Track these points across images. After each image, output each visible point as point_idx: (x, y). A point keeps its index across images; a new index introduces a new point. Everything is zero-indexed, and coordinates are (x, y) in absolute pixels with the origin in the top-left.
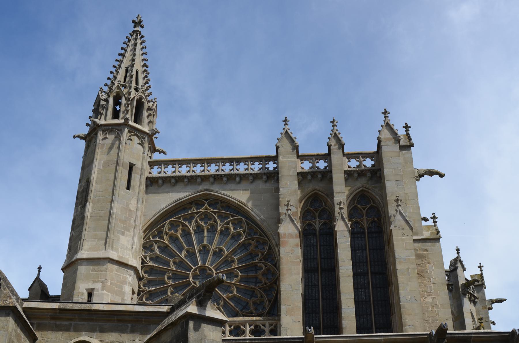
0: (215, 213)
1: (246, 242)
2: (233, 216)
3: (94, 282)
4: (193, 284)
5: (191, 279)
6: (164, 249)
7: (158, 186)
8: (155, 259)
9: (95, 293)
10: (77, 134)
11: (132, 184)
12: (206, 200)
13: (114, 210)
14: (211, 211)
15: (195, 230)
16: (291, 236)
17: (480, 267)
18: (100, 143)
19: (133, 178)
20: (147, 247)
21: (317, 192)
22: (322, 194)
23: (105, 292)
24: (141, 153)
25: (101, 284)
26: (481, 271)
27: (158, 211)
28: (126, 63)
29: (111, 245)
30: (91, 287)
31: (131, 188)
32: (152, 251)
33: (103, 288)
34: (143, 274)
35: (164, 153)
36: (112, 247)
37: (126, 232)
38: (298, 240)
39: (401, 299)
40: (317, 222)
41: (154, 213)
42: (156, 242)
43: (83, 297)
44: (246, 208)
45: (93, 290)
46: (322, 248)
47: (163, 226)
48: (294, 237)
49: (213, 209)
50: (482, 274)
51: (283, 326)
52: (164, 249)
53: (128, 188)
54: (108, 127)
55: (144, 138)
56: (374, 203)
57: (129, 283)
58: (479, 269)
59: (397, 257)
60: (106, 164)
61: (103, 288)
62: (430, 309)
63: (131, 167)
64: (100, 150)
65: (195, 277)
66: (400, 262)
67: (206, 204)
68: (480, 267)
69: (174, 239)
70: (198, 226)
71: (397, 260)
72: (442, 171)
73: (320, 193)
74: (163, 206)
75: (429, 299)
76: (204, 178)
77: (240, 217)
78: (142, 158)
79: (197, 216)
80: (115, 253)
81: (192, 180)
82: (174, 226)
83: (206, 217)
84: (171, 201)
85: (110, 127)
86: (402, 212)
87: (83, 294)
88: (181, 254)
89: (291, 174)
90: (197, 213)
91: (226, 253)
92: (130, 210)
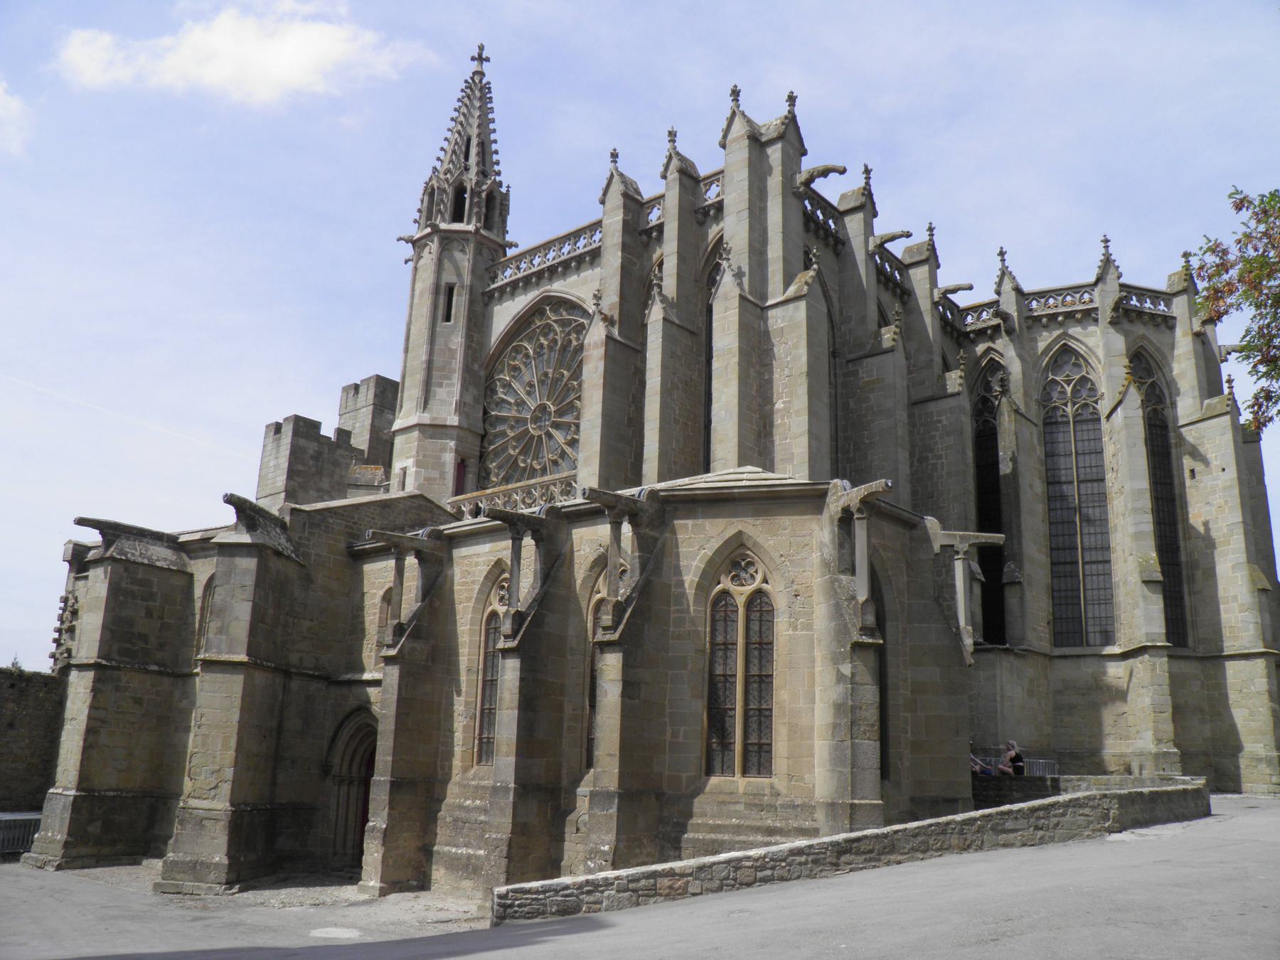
3: (407, 458)
14: (554, 321)
16: (596, 346)
31: (453, 317)
35: (516, 246)
37: (445, 382)
38: (602, 351)
45: (406, 468)
47: (505, 357)
53: (448, 318)
55: (468, 240)
57: (451, 449)
70: (541, 346)
72: (839, 163)
76: (539, 275)
77: (582, 320)
79: (538, 331)
81: (527, 282)
82: (517, 350)
84: (512, 316)
92: (450, 350)
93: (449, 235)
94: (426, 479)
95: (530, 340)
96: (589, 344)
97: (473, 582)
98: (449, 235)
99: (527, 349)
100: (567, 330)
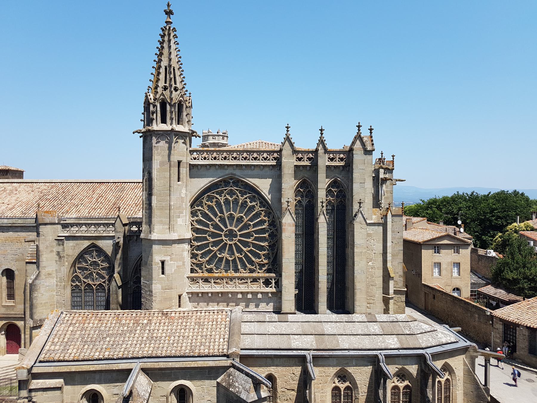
0: (237, 190)
1: (258, 213)
2: (249, 193)
3: (165, 255)
4: (225, 241)
5: (224, 238)
6: (205, 215)
7: (198, 169)
8: (199, 222)
9: (166, 263)
10: (135, 130)
11: (181, 177)
12: (231, 179)
13: (172, 203)
15: (224, 202)
16: (289, 225)
17: (393, 156)
18: (155, 146)
19: (181, 172)
20: (193, 214)
21: (306, 178)
22: (310, 181)
23: (172, 262)
24: (185, 149)
25: (169, 257)
26: (393, 159)
27: (199, 188)
28: (164, 63)
29: (173, 229)
30: (163, 259)
31: (181, 179)
32: (197, 216)
33: (171, 260)
34: (193, 233)
36: (174, 231)
39: (355, 272)
40: (304, 200)
42: (199, 210)
43: (159, 266)
44: (258, 189)
46: (306, 218)
48: (292, 225)
49: (237, 187)
50: (393, 161)
51: (283, 286)
52: (205, 215)
54: (159, 132)
56: (342, 188)
57: (186, 249)
58: (392, 157)
59: (355, 243)
60: (162, 164)
61: (171, 260)
62: (370, 270)
63: (179, 162)
64: (156, 151)
65: (226, 236)
66: (357, 247)
67: (231, 183)
68: (393, 156)
69: (210, 208)
70: (227, 199)
71: (355, 245)
73: (307, 180)
74: (202, 185)
75: (370, 263)
78: (186, 153)
80: (176, 234)
83: (231, 193)
85: (161, 132)
86: (362, 212)
87: (158, 263)
88: (216, 218)
89: (290, 173)
90: (226, 190)
91: (246, 220)
92: (182, 197)
93: (178, 133)
94: (177, 267)
95: (220, 194)
96: (285, 223)
97: (328, 376)
98: (178, 133)
99: (217, 198)
100: (245, 196)
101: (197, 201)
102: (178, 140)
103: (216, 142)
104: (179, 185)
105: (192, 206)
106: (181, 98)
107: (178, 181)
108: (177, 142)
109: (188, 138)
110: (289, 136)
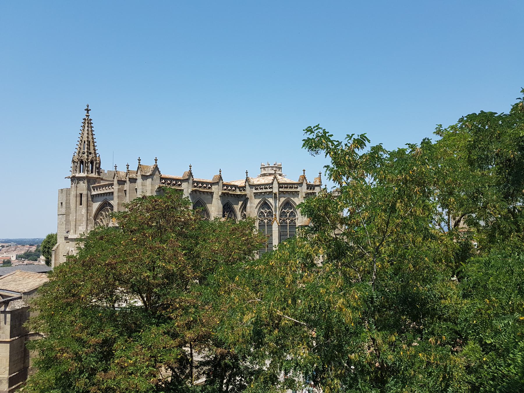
41: (95, 210)
53: (81, 205)
63: (81, 194)
92: (82, 214)
101: (96, 217)
102: (79, 182)
103: (266, 173)
104: (80, 207)
105: (95, 220)
106: (82, 158)
107: (81, 205)
108: (79, 183)
109: (86, 180)
110: (116, 172)
